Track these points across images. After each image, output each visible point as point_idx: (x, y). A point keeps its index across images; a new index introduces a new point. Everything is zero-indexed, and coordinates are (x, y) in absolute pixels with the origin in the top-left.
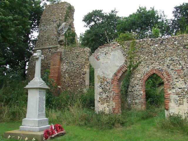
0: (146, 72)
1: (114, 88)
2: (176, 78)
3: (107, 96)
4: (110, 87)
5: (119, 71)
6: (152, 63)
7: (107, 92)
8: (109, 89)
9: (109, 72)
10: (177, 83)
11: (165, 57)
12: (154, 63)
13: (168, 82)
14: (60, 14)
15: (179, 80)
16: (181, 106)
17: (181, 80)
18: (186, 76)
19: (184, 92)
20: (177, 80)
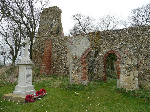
0: (106, 52)
1: (82, 64)
2: (125, 57)
3: (78, 69)
4: (79, 63)
5: (85, 52)
6: (111, 46)
7: (78, 66)
8: (79, 64)
9: (79, 52)
10: (126, 61)
11: (120, 42)
12: (112, 46)
13: (119, 60)
14: (52, 15)
15: (127, 59)
16: (128, 77)
17: (128, 58)
18: (132, 56)
19: (130, 67)
20: (126, 59)
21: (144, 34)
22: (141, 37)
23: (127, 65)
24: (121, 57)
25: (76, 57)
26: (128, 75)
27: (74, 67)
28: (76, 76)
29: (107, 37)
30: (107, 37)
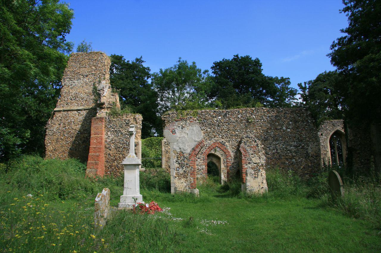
0: (208, 145)
1: (192, 163)
2: (252, 154)
3: (185, 171)
4: (187, 162)
5: (197, 147)
6: (215, 137)
7: (184, 168)
8: (187, 164)
9: (186, 146)
10: (253, 159)
11: (228, 131)
12: (217, 136)
13: (245, 158)
15: (255, 156)
16: (256, 179)
17: (256, 155)
18: (260, 152)
19: (258, 167)
20: (253, 156)
21: (261, 120)
22: (258, 124)
23: (255, 165)
24: (247, 154)
25: (182, 153)
26: (255, 177)
27: (178, 169)
28: (183, 183)
29: (209, 122)
30: (209, 122)
